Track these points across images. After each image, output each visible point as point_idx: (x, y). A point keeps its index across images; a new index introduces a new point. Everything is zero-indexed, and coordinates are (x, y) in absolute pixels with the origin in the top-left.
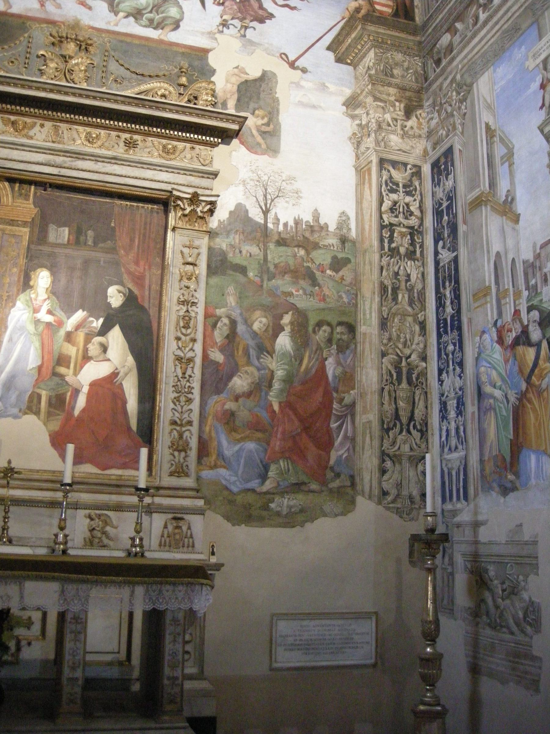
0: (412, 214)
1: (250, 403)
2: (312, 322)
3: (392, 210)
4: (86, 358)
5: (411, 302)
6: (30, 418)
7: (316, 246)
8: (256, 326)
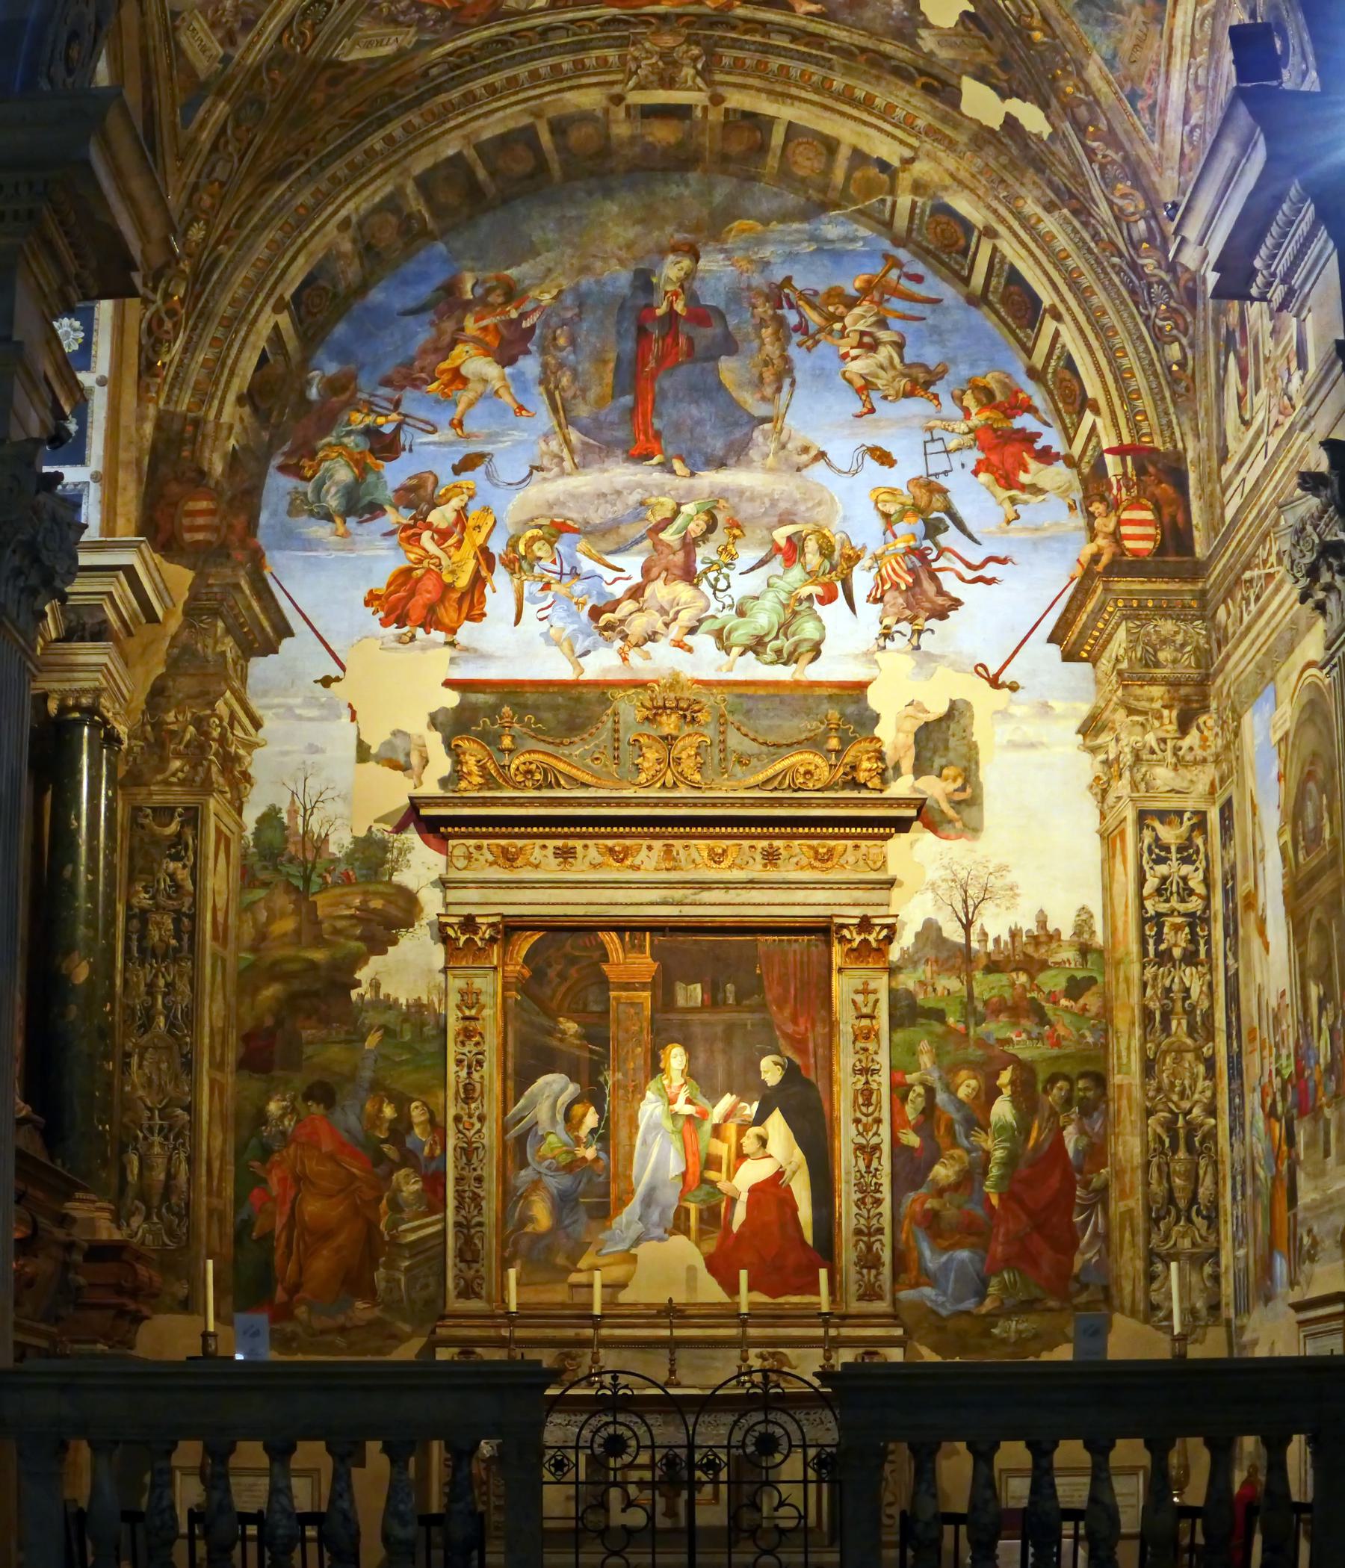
0: (1191, 892)
2: (1042, 1076)
3: (1159, 891)
4: (741, 1156)
5: (1191, 1031)
6: (680, 1240)
7: (1044, 966)
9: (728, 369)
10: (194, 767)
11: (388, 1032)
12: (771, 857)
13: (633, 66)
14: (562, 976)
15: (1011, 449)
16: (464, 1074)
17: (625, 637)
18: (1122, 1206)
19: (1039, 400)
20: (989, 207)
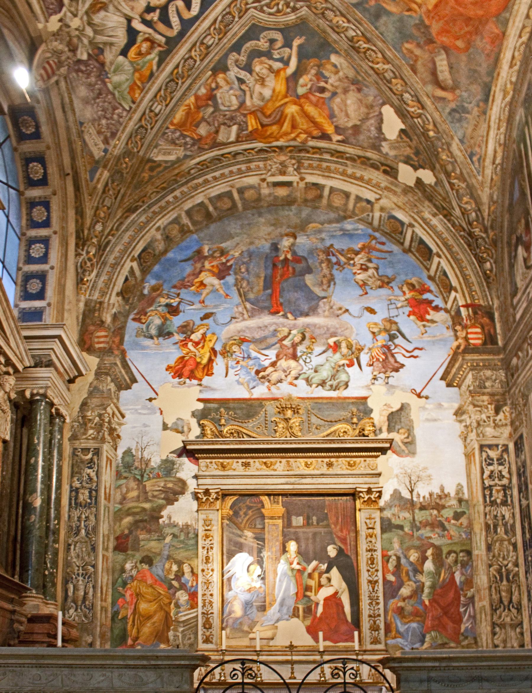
0: (503, 477)
1: (412, 602)
2: (445, 551)
3: (490, 477)
4: (320, 586)
5: (506, 533)
6: (295, 620)
7: (444, 507)
8: (412, 559)
9: (309, 279)
10: (98, 433)
11: (174, 536)
12: (330, 465)
13: (269, 168)
14: (246, 514)
15: (422, 306)
17: (269, 381)
18: (481, 604)
19: (433, 287)
20: (411, 216)
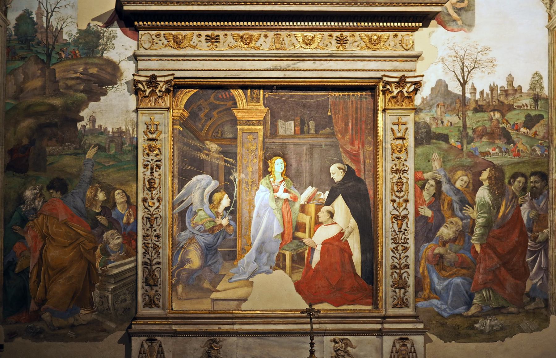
4: (318, 223)
7: (511, 108)
11: (101, 148)
16: (148, 173)
